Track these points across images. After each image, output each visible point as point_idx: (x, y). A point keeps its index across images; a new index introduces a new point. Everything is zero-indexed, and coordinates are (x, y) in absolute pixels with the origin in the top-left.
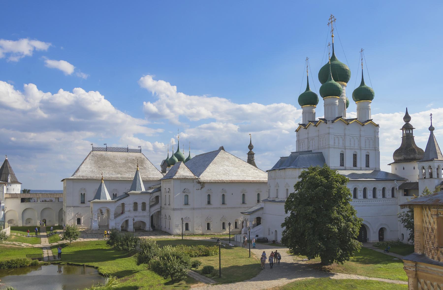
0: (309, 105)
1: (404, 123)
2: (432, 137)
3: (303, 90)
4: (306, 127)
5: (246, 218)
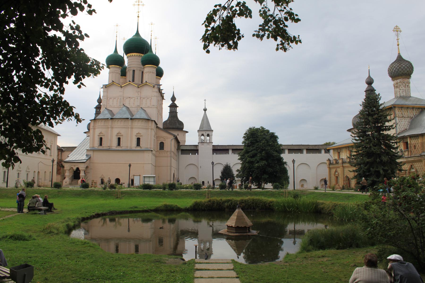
0: (118, 66)
1: (171, 102)
2: (205, 114)
3: (112, 52)
4: (122, 86)
5: (73, 166)
